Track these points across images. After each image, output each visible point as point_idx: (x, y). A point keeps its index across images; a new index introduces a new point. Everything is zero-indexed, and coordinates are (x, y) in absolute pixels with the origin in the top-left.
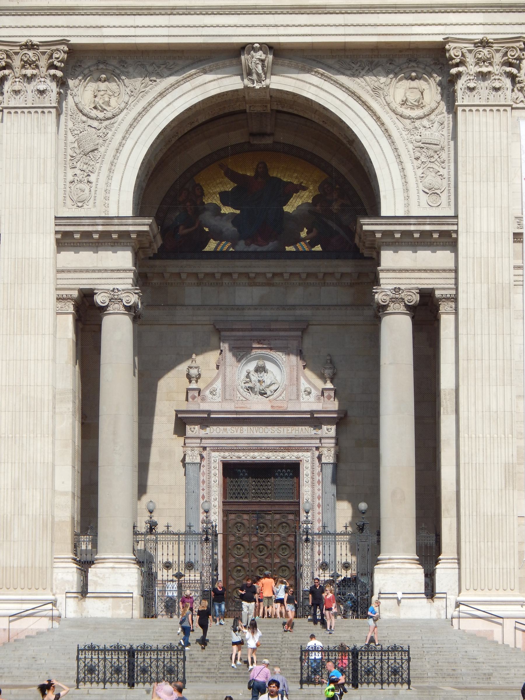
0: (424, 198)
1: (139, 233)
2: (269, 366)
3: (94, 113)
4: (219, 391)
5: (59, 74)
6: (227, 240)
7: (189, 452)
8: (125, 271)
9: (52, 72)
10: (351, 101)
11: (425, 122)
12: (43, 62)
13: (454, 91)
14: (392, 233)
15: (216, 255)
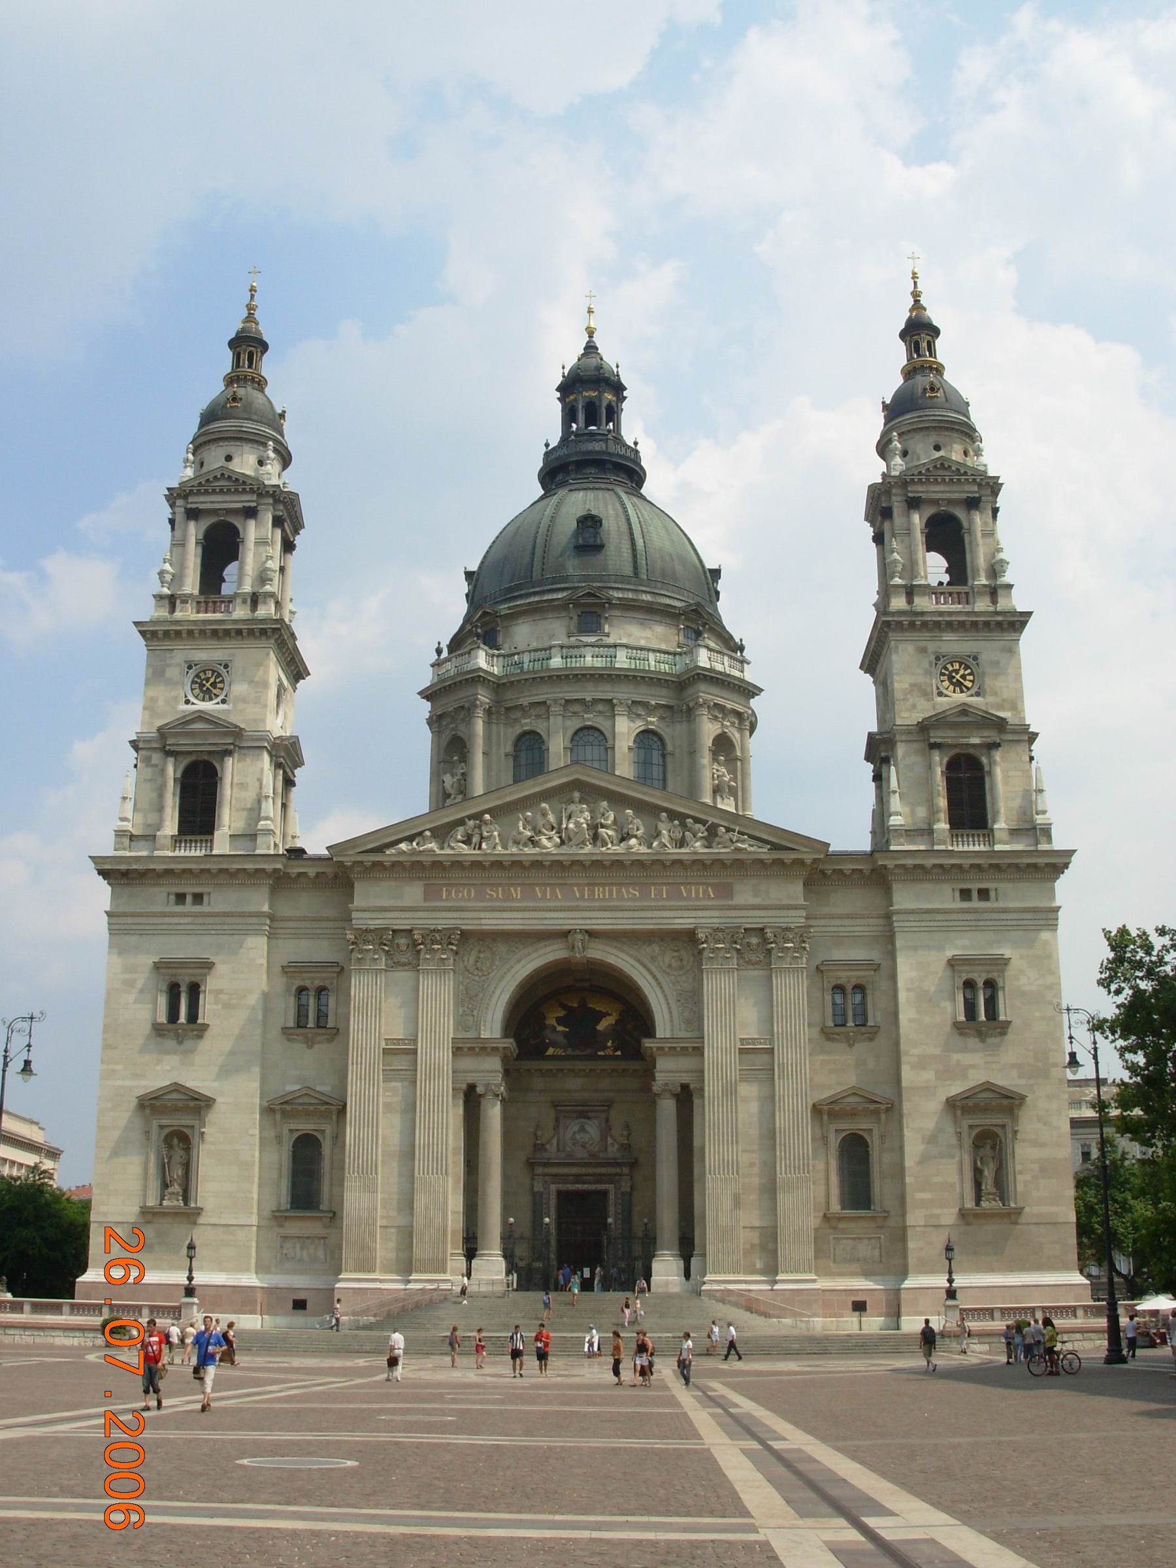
0: (683, 1026)
1: (504, 1048)
2: (588, 1128)
3: (476, 972)
4: (555, 1144)
5: (454, 948)
6: (560, 1047)
7: (536, 1184)
8: (496, 1072)
9: (450, 947)
10: (637, 965)
11: (684, 978)
12: (445, 942)
13: (701, 959)
14: (662, 1048)
15: (554, 1058)
